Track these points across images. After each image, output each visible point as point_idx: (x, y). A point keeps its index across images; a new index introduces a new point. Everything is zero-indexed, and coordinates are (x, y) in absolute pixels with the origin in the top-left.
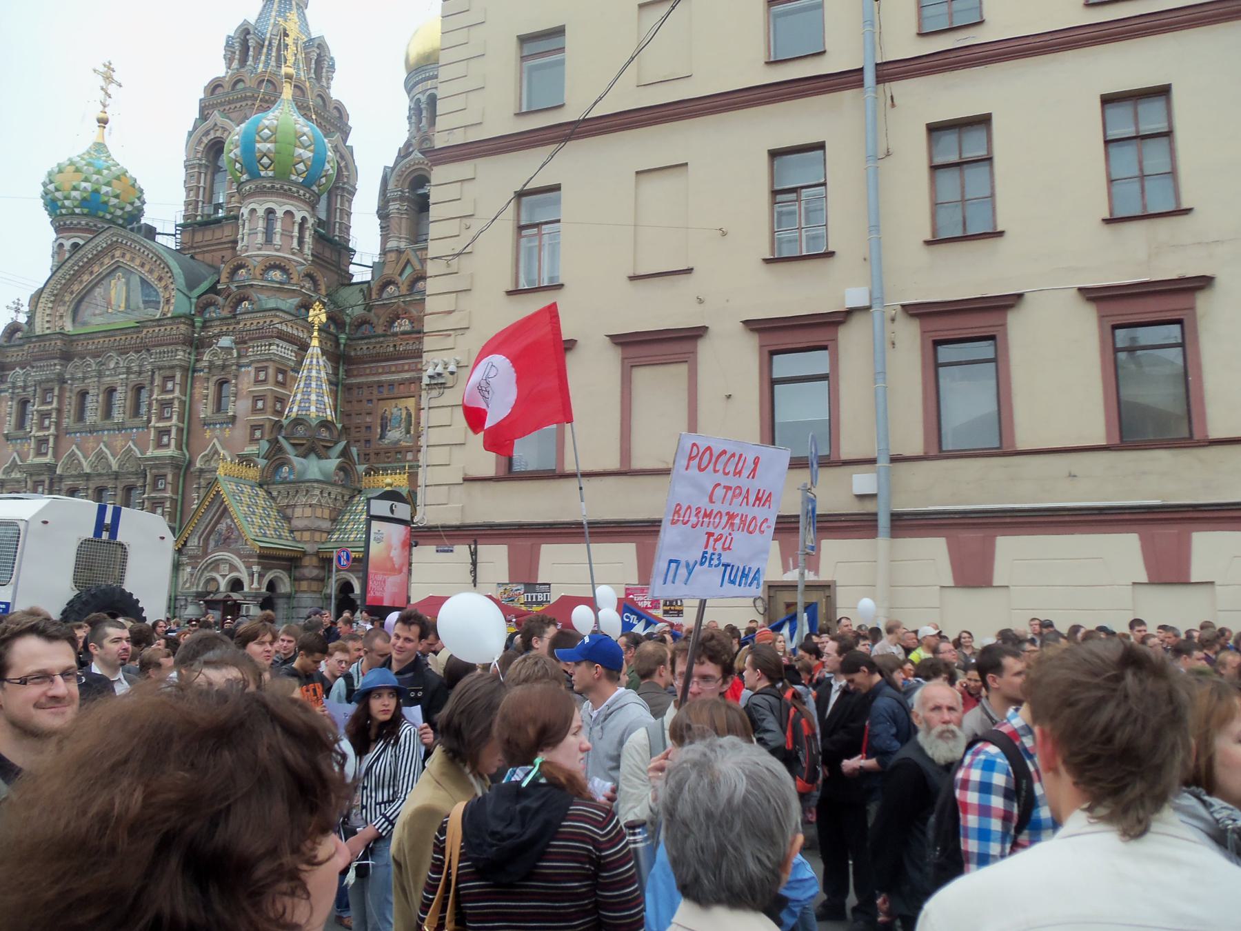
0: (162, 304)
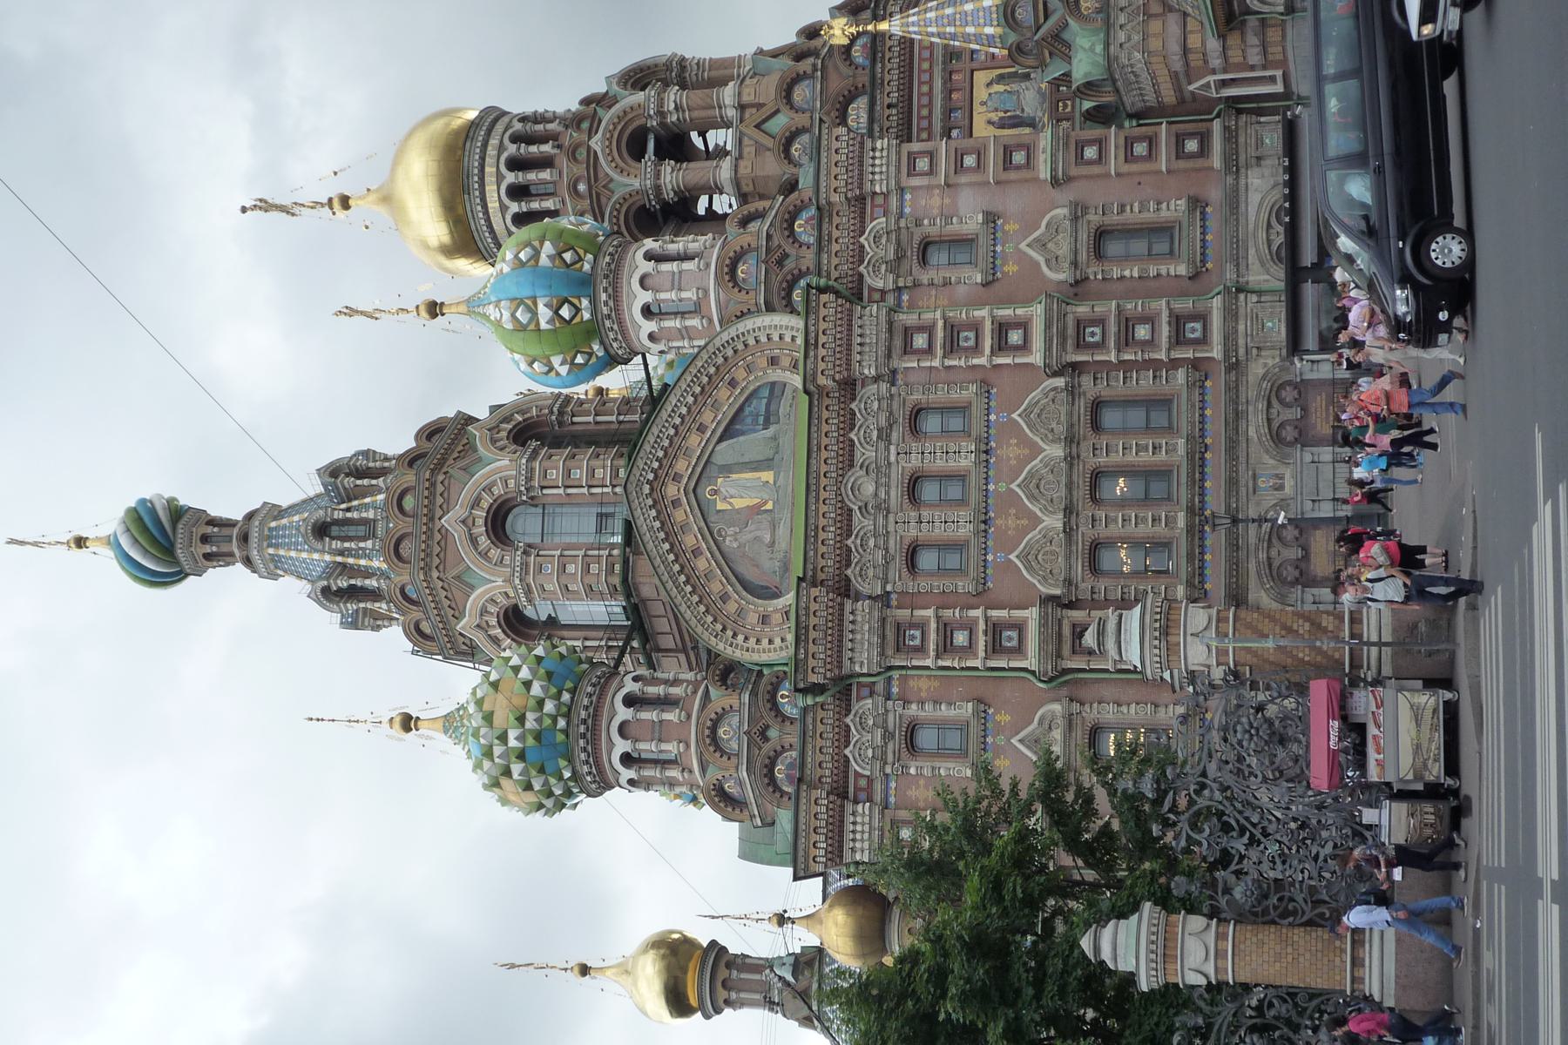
0: (776, 375)
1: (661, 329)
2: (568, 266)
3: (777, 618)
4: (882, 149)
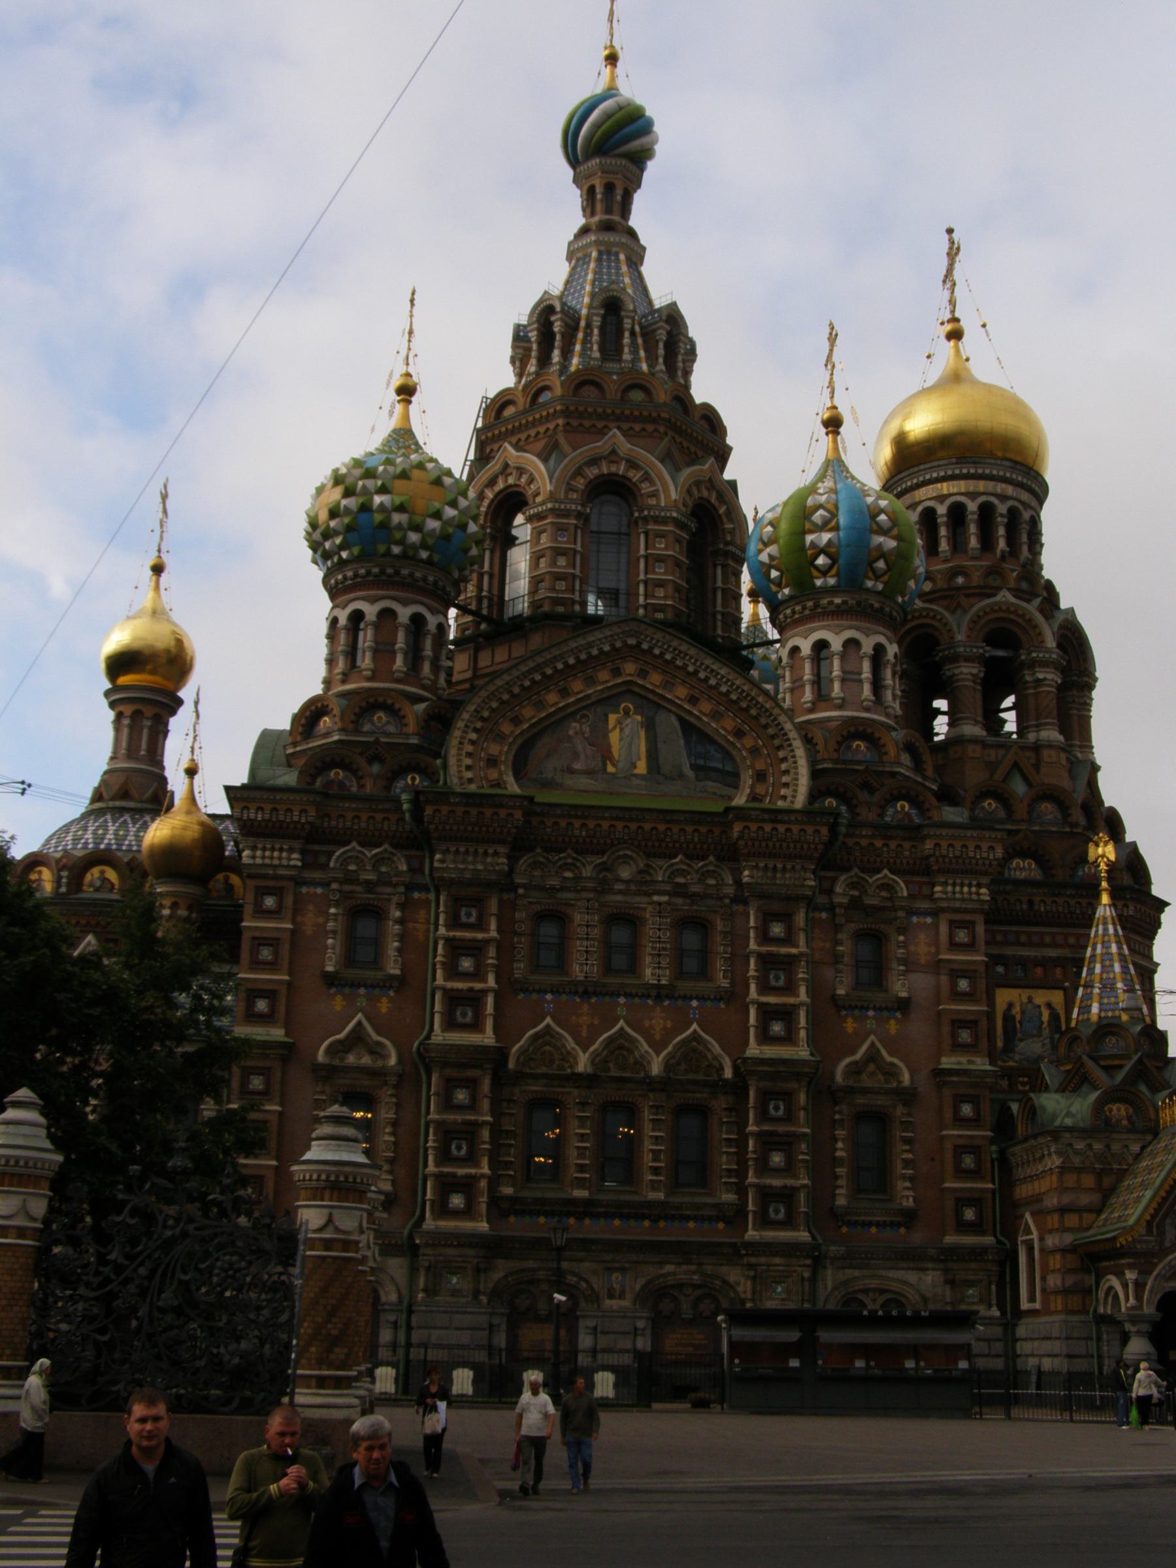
0: (747, 779)
1: (803, 659)
2: (871, 564)
3: (493, 774)
4: (978, 894)
